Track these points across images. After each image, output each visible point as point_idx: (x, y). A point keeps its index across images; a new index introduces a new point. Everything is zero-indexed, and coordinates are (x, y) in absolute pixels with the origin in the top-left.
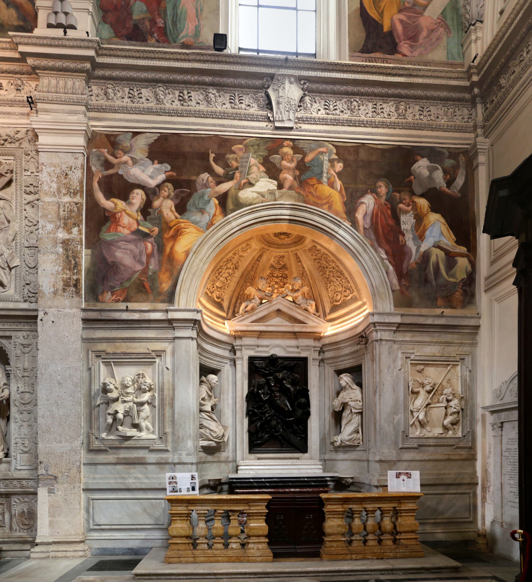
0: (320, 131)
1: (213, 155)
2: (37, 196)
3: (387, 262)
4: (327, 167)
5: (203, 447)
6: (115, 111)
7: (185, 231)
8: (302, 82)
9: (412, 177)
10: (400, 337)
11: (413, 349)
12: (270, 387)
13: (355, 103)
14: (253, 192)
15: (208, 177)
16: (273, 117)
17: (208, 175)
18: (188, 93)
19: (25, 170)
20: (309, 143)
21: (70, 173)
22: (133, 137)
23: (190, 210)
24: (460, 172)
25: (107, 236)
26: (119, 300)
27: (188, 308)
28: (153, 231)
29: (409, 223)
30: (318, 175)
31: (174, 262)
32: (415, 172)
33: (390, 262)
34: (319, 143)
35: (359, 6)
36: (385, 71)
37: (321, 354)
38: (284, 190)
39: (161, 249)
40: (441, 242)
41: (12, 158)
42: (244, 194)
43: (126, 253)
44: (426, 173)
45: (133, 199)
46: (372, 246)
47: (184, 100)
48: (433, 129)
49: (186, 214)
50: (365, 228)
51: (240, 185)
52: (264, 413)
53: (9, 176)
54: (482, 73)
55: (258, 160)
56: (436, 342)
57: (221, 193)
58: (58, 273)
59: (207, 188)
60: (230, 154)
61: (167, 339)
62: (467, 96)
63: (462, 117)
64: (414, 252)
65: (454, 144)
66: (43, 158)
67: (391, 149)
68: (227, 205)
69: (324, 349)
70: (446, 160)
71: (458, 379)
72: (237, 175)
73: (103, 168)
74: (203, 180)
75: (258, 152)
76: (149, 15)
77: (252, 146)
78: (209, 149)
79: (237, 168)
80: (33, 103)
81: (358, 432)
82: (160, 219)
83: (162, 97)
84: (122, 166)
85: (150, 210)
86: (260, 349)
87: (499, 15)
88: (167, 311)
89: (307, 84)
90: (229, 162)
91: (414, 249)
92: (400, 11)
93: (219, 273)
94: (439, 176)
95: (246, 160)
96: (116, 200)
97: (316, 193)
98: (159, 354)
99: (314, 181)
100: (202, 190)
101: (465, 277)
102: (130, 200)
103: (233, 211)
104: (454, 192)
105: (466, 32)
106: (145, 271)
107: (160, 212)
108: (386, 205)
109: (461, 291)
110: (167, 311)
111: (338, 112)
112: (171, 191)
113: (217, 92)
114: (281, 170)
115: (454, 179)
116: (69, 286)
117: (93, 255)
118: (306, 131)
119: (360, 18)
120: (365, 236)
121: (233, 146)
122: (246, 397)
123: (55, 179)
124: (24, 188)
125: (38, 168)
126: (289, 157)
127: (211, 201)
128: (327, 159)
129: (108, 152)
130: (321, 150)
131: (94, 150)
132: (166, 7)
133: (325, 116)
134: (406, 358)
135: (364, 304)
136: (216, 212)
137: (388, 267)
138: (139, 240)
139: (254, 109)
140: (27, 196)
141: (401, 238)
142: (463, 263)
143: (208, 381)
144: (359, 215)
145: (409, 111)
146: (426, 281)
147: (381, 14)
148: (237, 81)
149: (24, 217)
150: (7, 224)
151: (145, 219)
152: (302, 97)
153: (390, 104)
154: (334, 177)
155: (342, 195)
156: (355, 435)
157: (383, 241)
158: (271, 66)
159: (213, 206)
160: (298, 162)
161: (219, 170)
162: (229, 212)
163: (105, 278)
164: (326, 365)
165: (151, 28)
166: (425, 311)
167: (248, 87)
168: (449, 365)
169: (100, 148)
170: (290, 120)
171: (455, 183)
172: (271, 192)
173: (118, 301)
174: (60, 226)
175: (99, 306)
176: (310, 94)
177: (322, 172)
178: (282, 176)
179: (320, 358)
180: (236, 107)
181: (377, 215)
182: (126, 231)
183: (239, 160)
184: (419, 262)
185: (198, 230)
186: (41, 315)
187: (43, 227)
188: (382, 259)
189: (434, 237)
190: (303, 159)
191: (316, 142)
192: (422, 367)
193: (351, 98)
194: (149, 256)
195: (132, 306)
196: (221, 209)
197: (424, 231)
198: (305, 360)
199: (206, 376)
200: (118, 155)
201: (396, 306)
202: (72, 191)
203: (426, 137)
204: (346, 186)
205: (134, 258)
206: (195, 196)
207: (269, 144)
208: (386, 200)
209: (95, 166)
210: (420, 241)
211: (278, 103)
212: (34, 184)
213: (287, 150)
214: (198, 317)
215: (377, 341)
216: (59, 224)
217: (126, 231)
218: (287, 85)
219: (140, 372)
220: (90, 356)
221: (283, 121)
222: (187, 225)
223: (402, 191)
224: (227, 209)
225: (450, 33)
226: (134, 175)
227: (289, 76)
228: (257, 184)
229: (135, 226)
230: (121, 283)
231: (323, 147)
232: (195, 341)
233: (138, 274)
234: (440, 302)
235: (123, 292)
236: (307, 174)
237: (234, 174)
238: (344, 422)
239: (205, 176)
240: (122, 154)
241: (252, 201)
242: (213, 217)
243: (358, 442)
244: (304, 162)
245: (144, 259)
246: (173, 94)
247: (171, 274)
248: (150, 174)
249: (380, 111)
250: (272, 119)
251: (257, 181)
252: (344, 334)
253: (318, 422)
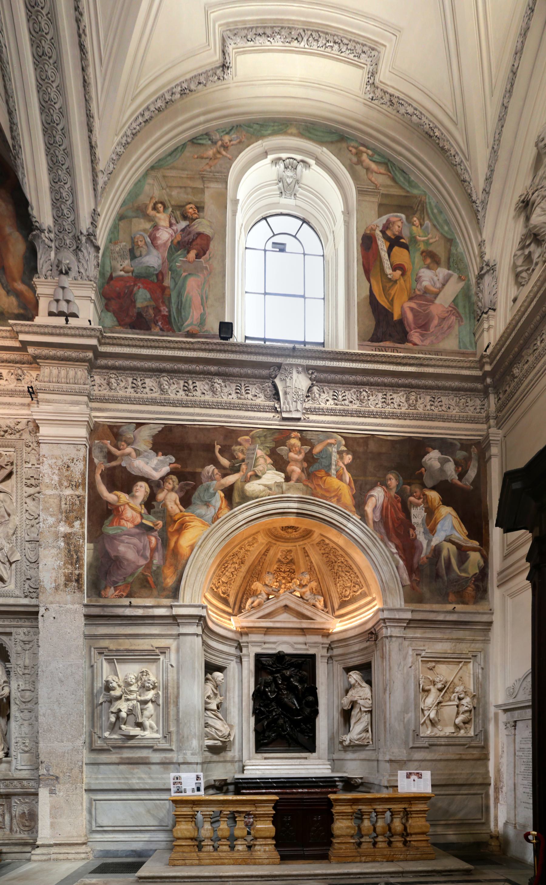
0: (328, 422)
1: (219, 447)
2: (38, 489)
3: (397, 556)
5: (208, 746)
6: (119, 402)
8: (310, 372)
9: (423, 469)
10: (410, 633)
11: (424, 646)
12: (277, 684)
13: (364, 393)
16: (280, 407)
18: (193, 383)
19: (26, 462)
21: (71, 465)
22: (136, 428)
24: (472, 464)
25: (110, 530)
26: (122, 595)
27: (193, 603)
28: (157, 525)
29: (420, 516)
30: (326, 467)
31: (179, 557)
32: (426, 464)
33: (400, 557)
34: (327, 434)
35: (368, 293)
36: (395, 360)
37: (330, 651)
38: (292, 483)
39: (165, 542)
40: (453, 536)
41: (13, 449)
43: (129, 547)
44: (437, 465)
45: (136, 492)
46: (382, 540)
47: (189, 390)
48: (444, 420)
49: (190, 507)
50: (374, 522)
51: (246, 477)
52: (271, 712)
53: (9, 468)
54: (495, 362)
56: (448, 639)
57: (227, 486)
58: (59, 567)
61: (171, 635)
62: (479, 386)
63: (474, 407)
64: (425, 546)
65: (466, 435)
66: (44, 449)
67: (401, 440)
68: (233, 498)
69: (333, 646)
70: (458, 452)
71: (470, 677)
72: (244, 467)
73: (105, 460)
74: (208, 473)
75: (265, 443)
76: (153, 303)
77: (259, 437)
78: (214, 440)
79: (243, 460)
80: (34, 393)
81: (368, 731)
82: (164, 512)
83: (167, 387)
84: (125, 458)
85: (154, 503)
86: (267, 646)
87: (512, 303)
88: (171, 607)
89: (315, 374)
91: (425, 543)
92: (411, 299)
93: (225, 568)
94: (451, 468)
95: (252, 452)
96: (119, 493)
98: (164, 651)
99: (322, 474)
101: (478, 571)
102: (134, 493)
103: (240, 504)
104: (466, 484)
105: (478, 320)
106: (149, 566)
107: (165, 505)
108: (396, 498)
109: (473, 586)
110: (171, 607)
111: (347, 402)
112: (175, 484)
113: (224, 382)
114: (289, 462)
115: (466, 472)
116: (71, 581)
117: (95, 549)
118: (314, 422)
119: (369, 307)
120: (375, 529)
122: (253, 695)
123: (57, 472)
124: (24, 481)
125: (39, 460)
126: (297, 448)
127: (217, 494)
129: (111, 444)
130: (330, 441)
131: (96, 441)
132: (170, 295)
133: (334, 406)
134: (417, 655)
135: (374, 600)
137: (398, 562)
138: (143, 534)
139: (260, 399)
140: (27, 488)
141: (411, 532)
142: (475, 557)
143: (213, 678)
144: (369, 509)
145: (420, 401)
146: (438, 576)
147: (391, 302)
148: (243, 371)
149: (24, 511)
150: (7, 518)
151: (149, 513)
152: (310, 387)
153: (401, 394)
155: (351, 488)
156: (364, 735)
158: (278, 356)
159: (219, 499)
160: (306, 454)
161: (225, 462)
162: (235, 505)
163: (107, 573)
164: (334, 662)
165: (155, 316)
166: (436, 607)
167: (255, 377)
168: (461, 662)
169: (103, 439)
170: (297, 410)
171: (467, 476)
172: (279, 485)
173: (121, 597)
174: (61, 520)
175: (102, 602)
176: (318, 384)
177: (330, 465)
178: (290, 468)
179: (329, 655)
180: (242, 397)
181: (387, 508)
182: (130, 525)
183: (245, 451)
184: (430, 556)
185: (204, 524)
186: (42, 611)
187: (44, 520)
188: (392, 554)
189: (445, 531)
190: (311, 451)
191: (324, 434)
192: (433, 664)
193: (360, 388)
194: (153, 551)
195: (135, 601)
197: (435, 524)
198: (313, 657)
199: (211, 674)
200: (122, 447)
201: (406, 602)
202: (74, 483)
203: (437, 428)
205: (138, 552)
206: (200, 489)
207: (276, 435)
209: (97, 458)
210: (431, 535)
211: (286, 393)
212: (35, 477)
213: (295, 442)
214: (203, 613)
215: (387, 637)
216: (60, 517)
217: (130, 525)
218: (295, 374)
219: (144, 670)
220: (92, 653)
221: (290, 411)
223: (413, 484)
225: (462, 322)
226: (137, 467)
227: (297, 366)
229: (138, 520)
230: (125, 578)
231: (332, 438)
232: (200, 638)
233: (141, 568)
234: (451, 597)
235: (127, 587)
236: (315, 466)
237: (240, 466)
238: (353, 721)
239: (211, 468)
240: (125, 445)
241: (258, 493)
243: (367, 741)
245: (148, 554)
246: (178, 383)
247: (176, 569)
248: (153, 466)
249: (390, 402)
250: (279, 410)
251: (264, 474)
252: (353, 631)
253: (326, 720)
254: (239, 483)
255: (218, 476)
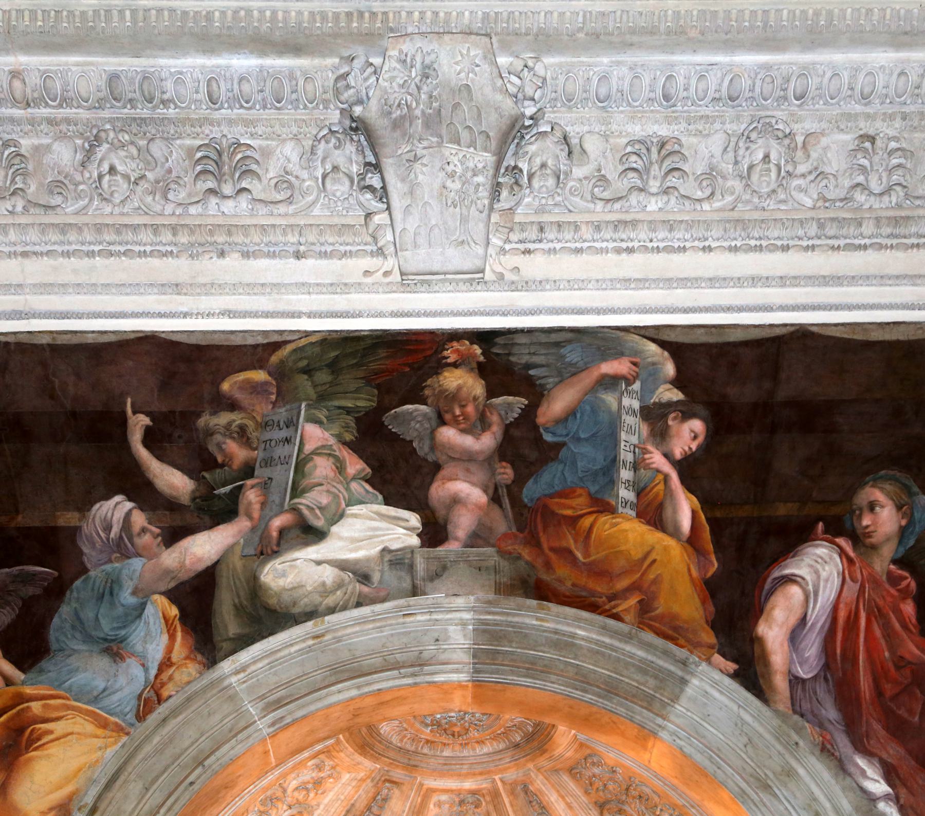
1: (144, 420)
4: (634, 440)
7: (51, 732)
14: (319, 563)
15: (128, 514)
17: (129, 505)
20: (558, 345)
23: (61, 650)
38: (452, 547)
42: (284, 575)
46: (826, 750)
49: (44, 664)
50: (795, 681)
55: (336, 431)
57: (184, 576)
59: (126, 555)
60: (214, 413)
68: (217, 620)
72: (252, 496)
74: (108, 528)
78: (123, 396)
79: (248, 471)
90: (212, 448)
95: (284, 434)
97: (587, 554)
99: (580, 503)
100: (108, 567)
103: (244, 642)
108: (893, 580)
114: (437, 467)
121: (223, 380)
126: (470, 409)
127: (149, 610)
128: (636, 405)
130: (609, 367)
136: (169, 650)
154: (666, 478)
157: (877, 726)
160: (508, 429)
162: (226, 646)
177: (613, 463)
183: (254, 435)
185: (104, 724)
190: (529, 413)
196: (191, 641)
204: (718, 514)
207: (380, 360)
208: (894, 561)
222: (57, 708)
224: (217, 638)
228: (334, 529)
231: (619, 354)
237: (236, 494)
241: (317, 599)
242: (161, 670)
244: (536, 427)
251: (339, 516)
254: (237, 562)
255: (147, 538)
